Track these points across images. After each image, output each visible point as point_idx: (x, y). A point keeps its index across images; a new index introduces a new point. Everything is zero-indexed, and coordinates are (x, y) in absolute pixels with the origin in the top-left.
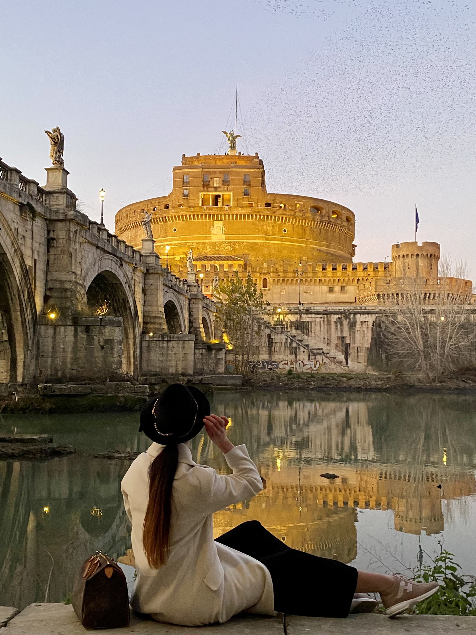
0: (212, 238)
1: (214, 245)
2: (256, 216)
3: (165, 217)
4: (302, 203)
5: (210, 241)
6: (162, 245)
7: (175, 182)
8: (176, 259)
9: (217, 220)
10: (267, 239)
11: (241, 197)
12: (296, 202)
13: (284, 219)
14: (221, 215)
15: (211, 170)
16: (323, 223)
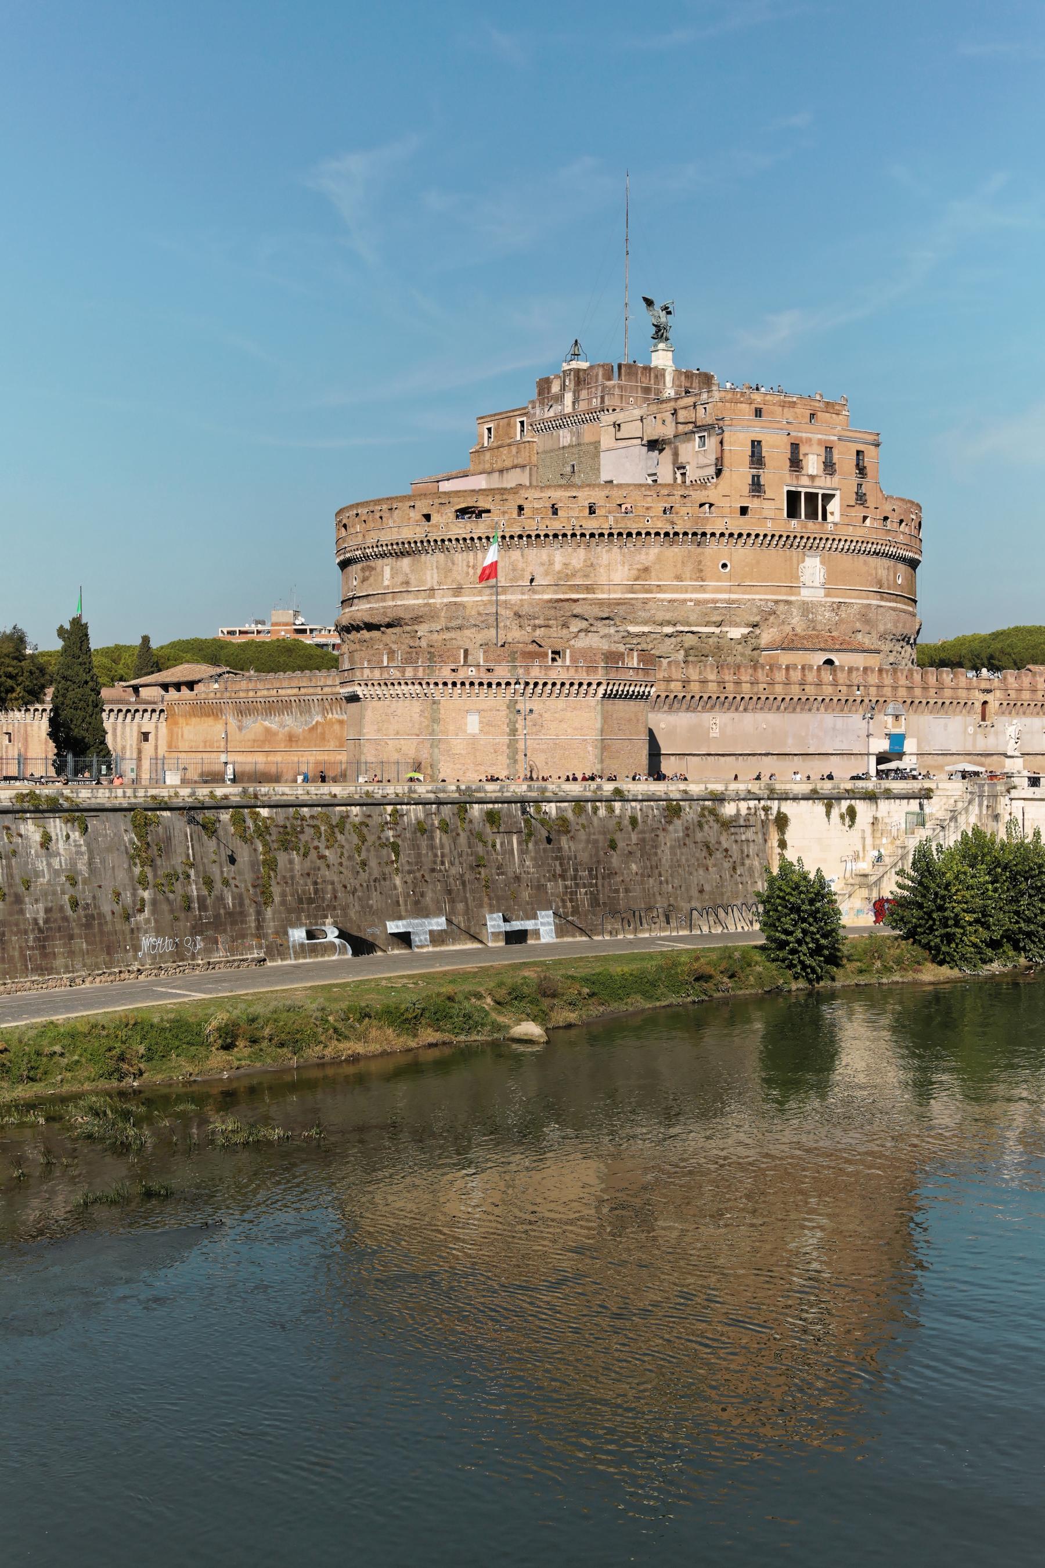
0: (804, 592)
1: (806, 608)
6: (691, 600)
8: (730, 636)
11: (853, 504)
15: (804, 435)
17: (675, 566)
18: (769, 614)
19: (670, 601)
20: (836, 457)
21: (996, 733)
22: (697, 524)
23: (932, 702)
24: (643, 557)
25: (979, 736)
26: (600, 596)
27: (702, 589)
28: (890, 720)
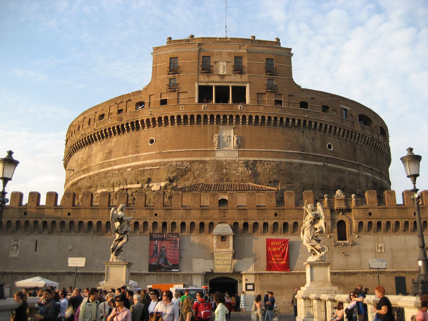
1: (219, 166)
2: (288, 119)
3: (137, 122)
4: (349, 109)
5: (213, 158)
6: (130, 167)
7: (155, 68)
8: (153, 189)
9: (224, 123)
10: (305, 157)
11: (264, 91)
12: (341, 106)
13: (328, 127)
14: (231, 117)
15: (215, 50)
16: (374, 140)
17: (124, 147)
18: (182, 172)
19: (119, 170)
20: (245, 62)
21: (359, 252)
22: (134, 116)
23: (271, 223)
24: (109, 144)
25: (335, 255)
26: (91, 173)
27: (137, 159)
28: (215, 241)
